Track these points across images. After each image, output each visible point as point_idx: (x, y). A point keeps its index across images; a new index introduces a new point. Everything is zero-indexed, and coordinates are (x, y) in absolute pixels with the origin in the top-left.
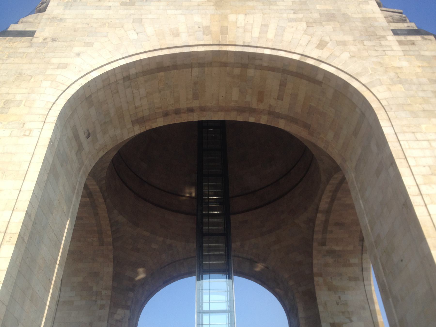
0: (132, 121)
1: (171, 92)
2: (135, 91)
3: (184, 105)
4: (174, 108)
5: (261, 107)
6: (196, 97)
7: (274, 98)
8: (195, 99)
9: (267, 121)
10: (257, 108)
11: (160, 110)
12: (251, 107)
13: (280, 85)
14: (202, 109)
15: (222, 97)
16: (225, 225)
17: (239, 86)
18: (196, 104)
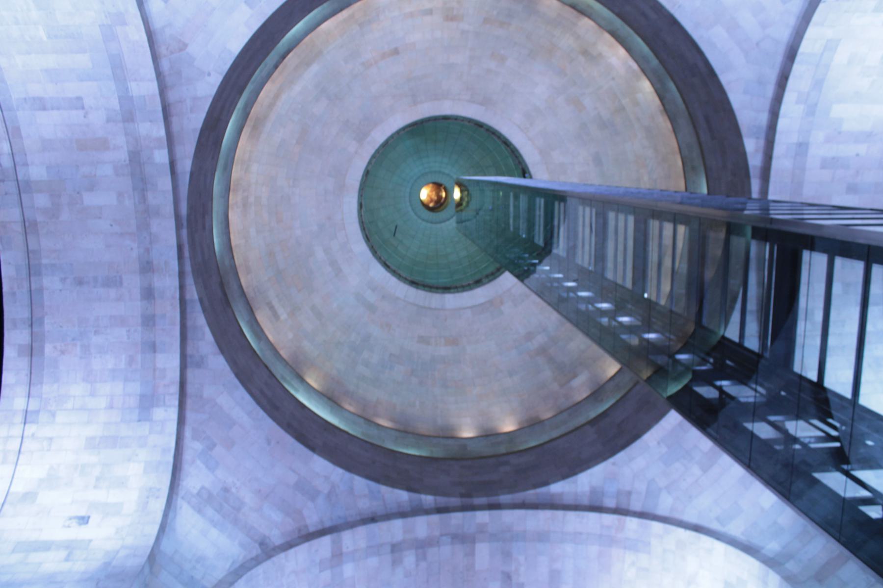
0: (139, 421)
1: (96, 333)
2: (69, 405)
3: (134, 307)
4: (140, 328)
5: (120, 140)
6: (113, 282)
7: (85, 117)
8: (121, 283)
9: (151, 121)
10: (125, 148)
11: (139, 357)
12: (127, 162)
13: (44, 109)
14: (147, 267)
15: (111, 225)
16: (512, 209)
17: (78, 193)
18: (133, 283)
